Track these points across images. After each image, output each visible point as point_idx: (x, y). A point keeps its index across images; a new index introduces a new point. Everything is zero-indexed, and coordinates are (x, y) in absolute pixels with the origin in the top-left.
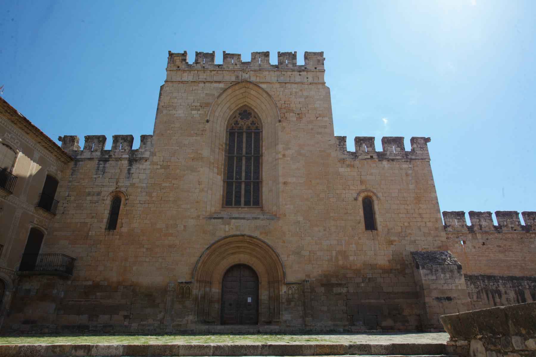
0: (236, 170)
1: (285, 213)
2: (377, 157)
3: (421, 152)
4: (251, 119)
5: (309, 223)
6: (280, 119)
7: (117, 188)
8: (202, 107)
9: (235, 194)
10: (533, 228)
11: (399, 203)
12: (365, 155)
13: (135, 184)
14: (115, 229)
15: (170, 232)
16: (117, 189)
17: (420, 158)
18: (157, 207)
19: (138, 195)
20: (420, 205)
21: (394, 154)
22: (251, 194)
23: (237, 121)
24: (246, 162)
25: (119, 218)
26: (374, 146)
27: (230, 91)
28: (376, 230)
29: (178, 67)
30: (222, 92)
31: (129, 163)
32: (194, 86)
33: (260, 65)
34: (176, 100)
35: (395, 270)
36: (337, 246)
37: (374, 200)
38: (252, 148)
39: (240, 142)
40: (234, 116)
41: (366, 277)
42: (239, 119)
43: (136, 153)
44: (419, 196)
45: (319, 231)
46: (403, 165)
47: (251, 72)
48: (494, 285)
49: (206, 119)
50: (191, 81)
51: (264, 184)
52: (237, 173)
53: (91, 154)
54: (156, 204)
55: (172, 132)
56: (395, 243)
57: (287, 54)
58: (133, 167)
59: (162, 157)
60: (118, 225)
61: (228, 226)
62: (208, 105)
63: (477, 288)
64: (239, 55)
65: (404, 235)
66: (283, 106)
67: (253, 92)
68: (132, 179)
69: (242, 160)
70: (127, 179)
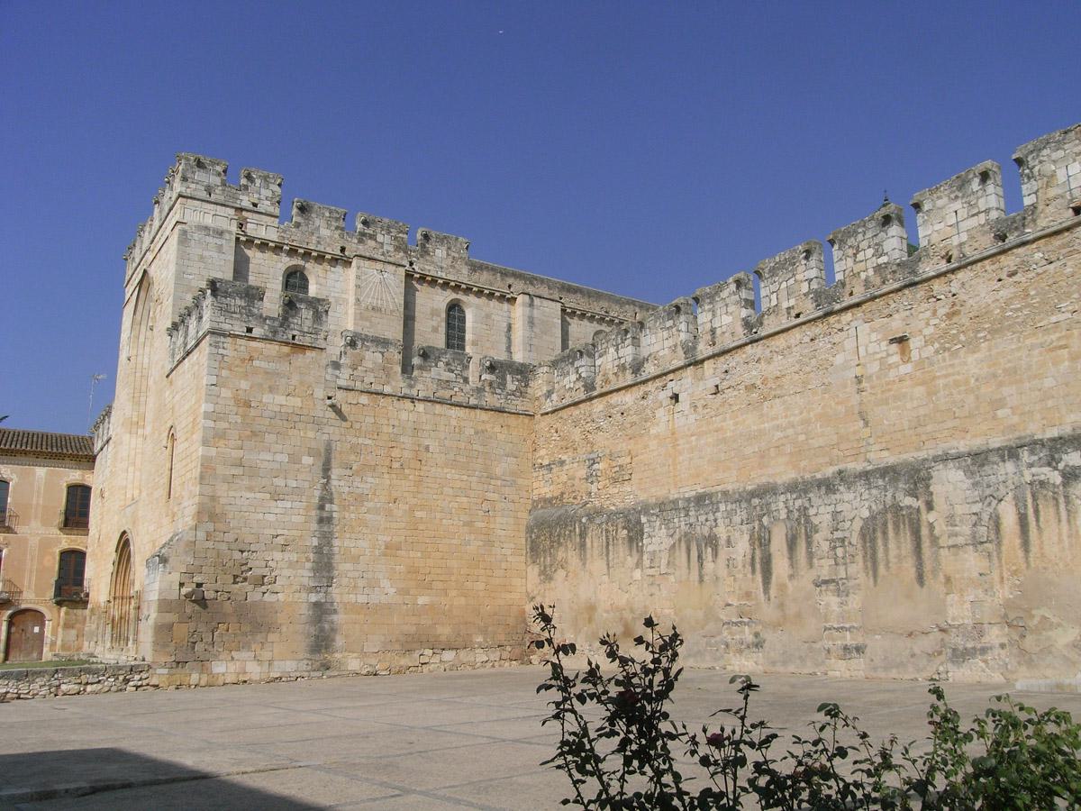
10: (848, 287)
48: (707, 520)
63: (672, 536)
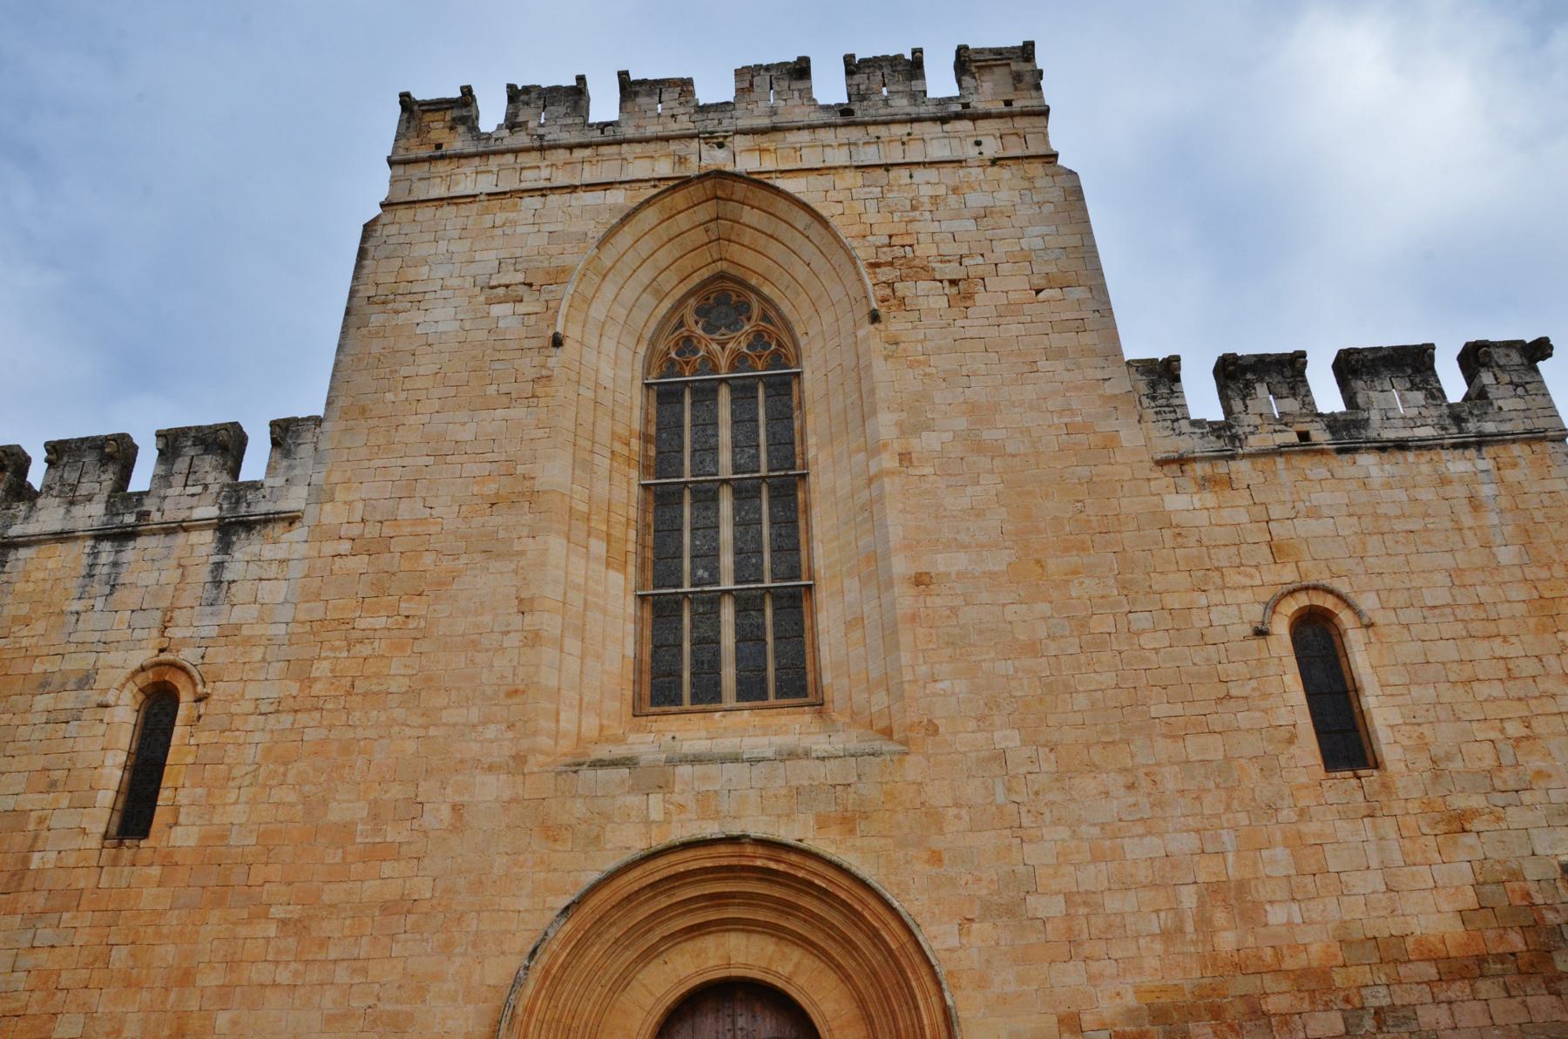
0: (693, 546)
1: (930, 721)
2: (1327, 436)
3: (1520, 404)
5: (1052, 756)
6: (875, 305)
7: (162, 651)
8: (530, 285)
9: (693, 652)
11: (1464, 633)
12: (1275, 431)
13: (239, 627)
14: (145, 834)
15: (388, 840)
16: (164, 657)
17: (1521, 428)
18: (330, 728)
19: (251, 676)
20: (1560, 635)
21: (1403, 418)
22: (766, 643)
23: (688, 339)
24: (736, 510)
25: (162, 785)
26: (1308, 393)
27: (650, 216)
28: (1377, 765)
29: (439, 146)
30: (614, 221)
31: (220, 540)
32: (501, 209)
33: (773, 112)
34: (427, 267)
35: (1501, 958)
36: (1198, 862)
37: (1345, 630)
38: (758, 446)
39: (706, 425)
40: (674, 321)
41: (1363, 1008)
42: (699, 331)
43: (249, 497)
44: (1547, 594)
45: (1107, 793)
46: (1450, 465)
47: (738, 137)
49: (551, 333)
50: (489, 194)
51: (822, 596)
52: (696, 556)
53: (68, 511)
54: (329, 710)
55: (403, 395)
56: (1476, 825)
57: (884, 64)
58: (237, 555)
59: (360, 505)
60: (161, 816)
61: (661, 795)
62: (558, 276)
64: (685, 86)
65: (1512, 785)
66: (883, 258)
67: (750, 216)
68: (226, 607)
69: (715, 499)
70: (209, 609)
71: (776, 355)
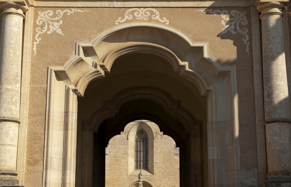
4: (144, 135)
67: (144, 125)
71: (146, 138)
